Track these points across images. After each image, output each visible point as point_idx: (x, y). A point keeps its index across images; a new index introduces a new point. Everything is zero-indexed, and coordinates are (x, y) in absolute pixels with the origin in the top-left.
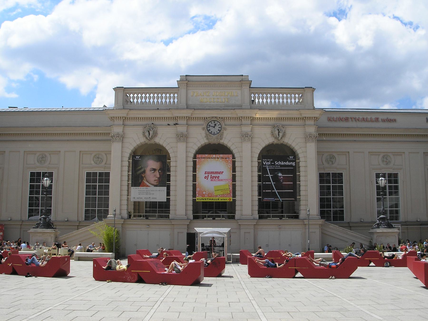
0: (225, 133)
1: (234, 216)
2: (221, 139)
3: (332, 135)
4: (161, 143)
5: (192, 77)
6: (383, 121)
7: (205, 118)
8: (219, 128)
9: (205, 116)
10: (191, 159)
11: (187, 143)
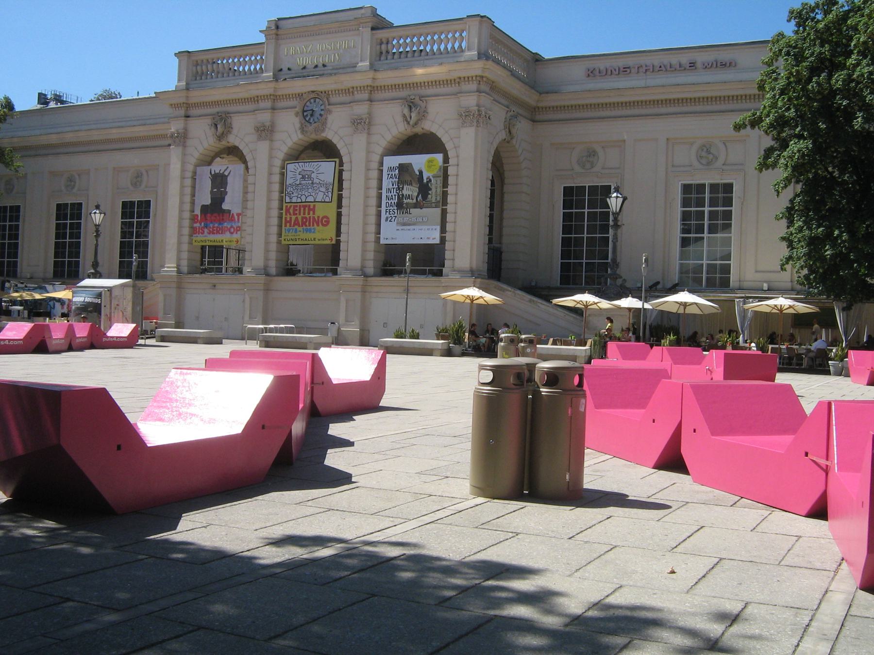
0: (330, 118)
1: (441, 271)
2: (323, 130)
3: (695, 100)
4: (330, 137)
5: (356, 11)
6: (708, 67)
7: (300, 95)
8: (322, 110)
9: (298, 90)
10: (277, 170)
11: (369, 134)
